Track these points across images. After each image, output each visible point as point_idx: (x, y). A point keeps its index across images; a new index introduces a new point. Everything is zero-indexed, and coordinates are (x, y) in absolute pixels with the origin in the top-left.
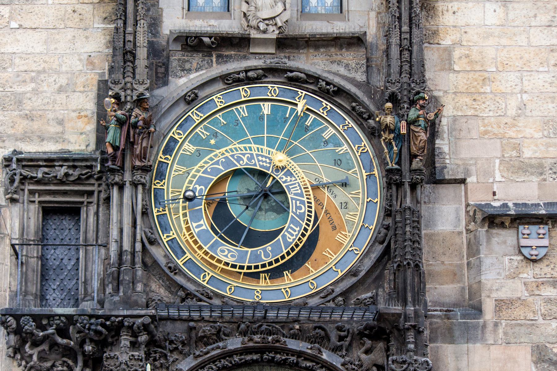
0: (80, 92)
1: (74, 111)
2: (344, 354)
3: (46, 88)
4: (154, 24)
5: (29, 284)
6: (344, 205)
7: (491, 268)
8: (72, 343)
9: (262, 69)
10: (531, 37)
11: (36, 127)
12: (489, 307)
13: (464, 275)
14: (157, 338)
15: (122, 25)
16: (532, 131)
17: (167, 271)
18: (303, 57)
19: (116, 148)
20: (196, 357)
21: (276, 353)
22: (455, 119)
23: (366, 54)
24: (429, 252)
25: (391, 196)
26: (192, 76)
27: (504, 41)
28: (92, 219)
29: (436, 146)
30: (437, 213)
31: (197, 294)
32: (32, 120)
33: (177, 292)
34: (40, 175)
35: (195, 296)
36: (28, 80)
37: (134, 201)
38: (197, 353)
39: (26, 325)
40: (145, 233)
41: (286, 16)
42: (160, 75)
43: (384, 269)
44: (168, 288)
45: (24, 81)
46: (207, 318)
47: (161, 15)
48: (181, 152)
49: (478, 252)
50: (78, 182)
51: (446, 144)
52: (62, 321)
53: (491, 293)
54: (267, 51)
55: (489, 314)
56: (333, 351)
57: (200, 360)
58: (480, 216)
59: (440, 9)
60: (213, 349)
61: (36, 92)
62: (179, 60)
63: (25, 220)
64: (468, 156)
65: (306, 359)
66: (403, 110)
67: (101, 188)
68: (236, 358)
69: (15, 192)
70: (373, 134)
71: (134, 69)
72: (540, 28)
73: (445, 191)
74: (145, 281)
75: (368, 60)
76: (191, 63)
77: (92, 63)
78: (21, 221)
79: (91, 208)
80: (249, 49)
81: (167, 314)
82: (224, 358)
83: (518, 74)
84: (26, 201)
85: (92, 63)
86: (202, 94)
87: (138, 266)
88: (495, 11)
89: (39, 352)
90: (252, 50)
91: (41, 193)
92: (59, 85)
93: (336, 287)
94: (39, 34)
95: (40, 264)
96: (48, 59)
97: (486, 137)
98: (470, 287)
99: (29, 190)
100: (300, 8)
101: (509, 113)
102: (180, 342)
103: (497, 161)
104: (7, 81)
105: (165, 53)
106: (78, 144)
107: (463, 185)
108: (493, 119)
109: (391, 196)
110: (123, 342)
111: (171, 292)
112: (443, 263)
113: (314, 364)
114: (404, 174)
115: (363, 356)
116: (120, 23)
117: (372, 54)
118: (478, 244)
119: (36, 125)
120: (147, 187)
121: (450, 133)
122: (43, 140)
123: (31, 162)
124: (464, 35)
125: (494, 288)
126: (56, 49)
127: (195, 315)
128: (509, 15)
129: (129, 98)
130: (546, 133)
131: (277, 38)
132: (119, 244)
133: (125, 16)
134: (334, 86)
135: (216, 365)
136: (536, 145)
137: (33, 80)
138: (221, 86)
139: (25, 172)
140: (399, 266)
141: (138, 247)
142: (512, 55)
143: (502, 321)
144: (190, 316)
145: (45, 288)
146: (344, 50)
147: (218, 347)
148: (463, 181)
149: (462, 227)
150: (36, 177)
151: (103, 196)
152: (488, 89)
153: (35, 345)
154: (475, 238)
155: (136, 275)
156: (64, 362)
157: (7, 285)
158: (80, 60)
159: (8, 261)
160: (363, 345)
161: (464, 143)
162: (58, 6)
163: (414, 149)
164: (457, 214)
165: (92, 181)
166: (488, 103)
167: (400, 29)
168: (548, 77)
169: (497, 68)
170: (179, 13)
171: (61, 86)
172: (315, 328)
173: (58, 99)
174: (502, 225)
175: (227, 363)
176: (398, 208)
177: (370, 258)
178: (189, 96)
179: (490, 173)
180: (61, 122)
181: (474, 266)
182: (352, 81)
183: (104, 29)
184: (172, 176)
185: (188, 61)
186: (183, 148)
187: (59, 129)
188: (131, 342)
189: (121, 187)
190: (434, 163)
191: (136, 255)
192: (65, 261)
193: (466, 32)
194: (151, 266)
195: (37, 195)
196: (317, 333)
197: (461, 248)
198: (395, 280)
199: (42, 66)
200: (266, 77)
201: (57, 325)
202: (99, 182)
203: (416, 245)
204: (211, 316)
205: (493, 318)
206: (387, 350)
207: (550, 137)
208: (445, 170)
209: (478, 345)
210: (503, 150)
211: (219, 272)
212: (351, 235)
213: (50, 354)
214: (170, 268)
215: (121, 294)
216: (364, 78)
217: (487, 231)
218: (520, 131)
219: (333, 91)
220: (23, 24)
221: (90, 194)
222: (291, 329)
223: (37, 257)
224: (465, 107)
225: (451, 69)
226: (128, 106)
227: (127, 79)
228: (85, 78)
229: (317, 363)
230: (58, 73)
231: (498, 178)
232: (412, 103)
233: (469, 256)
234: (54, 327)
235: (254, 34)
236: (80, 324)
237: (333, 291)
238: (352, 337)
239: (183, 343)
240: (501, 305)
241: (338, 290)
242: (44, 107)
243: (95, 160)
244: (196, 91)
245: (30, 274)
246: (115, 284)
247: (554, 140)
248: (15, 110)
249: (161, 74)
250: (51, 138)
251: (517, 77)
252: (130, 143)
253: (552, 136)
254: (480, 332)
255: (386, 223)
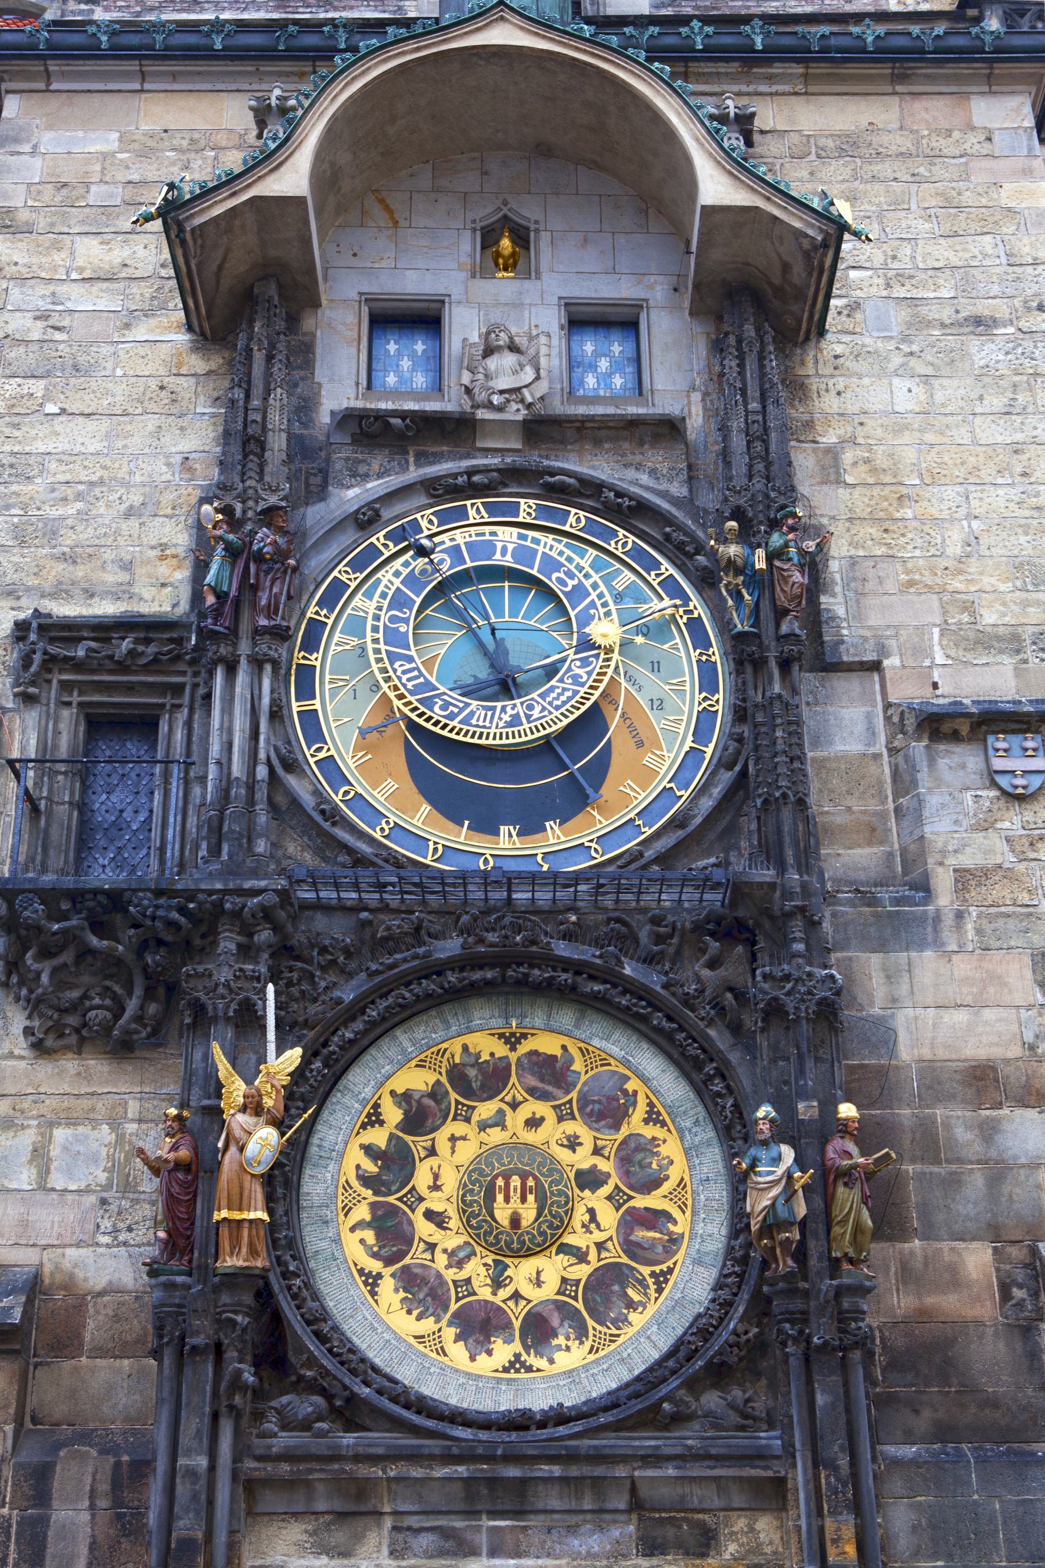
0: (166, 516)
1: (153, 548)
2: (667, 968)
3: (102, 510)
4: (304, 407)
5: (52, 852)
6: (656, 704)
7: (941, 813)
8: (120, 947)
9: (498, 470)
10: (978, 431)
11: (80, 574)
12: (943, 882)
13: (890, 830)
14: (294, 942)
15: (242, 396)
16: (993, 580)
17: (318, 818)
18: (573, 457)
19: (221, 597)
20: (372, 974)
21: (531, 966)
22: (853, 562)
23: (687, 454)
24: (821, 791)
25: (744, 683)
26: (369, 485)
27: (930, 437)
28: (179, 735)
29: (823, 606)
30: (832, 721)
31: (375, 859)
32: (75, 562)
33: (336, 857)
34: (81, 653)
35: (373, 864)
36: (71, 497)
37: (256, 692)
38: (374, 967)
39: (26, 909)
40: (276, 749)
41: (542, 388)
42: (313, 488)
43: (739, 814)
44: (318, 852)
45: (65, 499)
46: (394, 905)
47: (319, 394)
48: (349, 611)
49: (914, 783)
50: (152, 668)
51: (839, 604)
52: (99, 902)
53: (945, 857)
54: (507, 446)
55: (944, 898)
56: (644, 961)
57: (378, 979)
58: (913, 720)
59: (814, 388)
60: (405, 960)
61: (83, 516)
62: (347, 459)
63: (50, 734)
64: (882, 623)
65: (592, 978)
66: (758, 536)
67: (196, 680)
68: (452, 977)
69: (33, 683)
70: (703, 580)
71: (262, 466)
72: (992, 417)
73: (846, 685)
74: (273, 837)
75: (690, 467)
76: (369, 465)
77: (190, 469)
78: (42, 737)
79: (179, 715)
80: (474, 442)
81: (313, 895)
82: (426, 977)
83: (960, 489)
84: (52, 701)
85: (190, 469)
86: (386, 514)
87: (261, 807)
88: (910, 391)
89: (55, 971)
90: (479, 444)
91: (83, 687)
92: (127, 504)
93: (648, 849)
94: (96, 423)
95: (66, 805)
96: (109, 464)
97: (912, 590)
98: (904, 851)
99: (60, 681)
100: (566, 384)
101: (949, 551)
102: (341, 949)
103: (936, 631)
104: (31, 498)
105: (323, 454)
106: (156, 603)
107: (876, 677)
108: (921, 562)
109: (744, 683)
110: (222, 945)
111: (325, 859)
112: (849, 809)
113: (608, 986)
114: (767, 643)
115: (706, 973)
116: (239, 394)
117: (698, 458)
118: (914, 769)
119: (80, 572)
120: (283, 671)
121: (846, 586)
122: (92, 596)
123: (68, 631)
124: (860, 428)
125: (950, 848)
126: (125, 446)
127: (372, 898)
128: (936, 397)
129: (250, 514)
130: (1018, 583)
131: (525, 421)
132: (225, 771)
133: (249, 382)
134: (631, 499)
135: (411, 991)
136: (1004, 604)
137: (79, 497)
138: (424, 500)
139: (53, 650)
140: (766, 802)
141: (262, 772)
142: (946, 459)
143: (971, 909)
144: (360, 899)
145: (86, 864)
146: (646, 447)
147: (416, 957)
148: (875, 666)
149: (880, 745)
150: (73, 658)
151: (202, 691)
152: (909, 513)
153: (45, 953)
154: (906, 762)
155: (255, 823)
156: (107, 989)
157: (7, 851)
158: (168, 465)
159: (11, 809)
160: (704, 951)
161: (871, 601)
162: (134, 379)
163: (782, 600)
164: (870, 722)
165: (182, 667)
166: (910, 536)
167: (746, 404)
168: (1014, 493)
169: (922, 480)
170: (351, 392)
171: (131, 507)
172: (609, 920)
173: (124, 526)
174: (955, 737)
175: (433, 987)
176: (759, 698)
177: (711, 796)
178: (364, 514)
179: (922, 650)
180: (127, 566)
181: (910, 814)
182: (664, 495)
183: (213, 415)
184: (331, 653)
185: (363, 461)
186: (352, 605)
187: (123, 577)
188: (239, 946)
189: (231, 670)
190: (820, 635)
191: (257, 787)
192: (127, 815)
193: (861, 424)
194: (287, 810)
195: (75, 693)
196: (612, 930)
197: (880, 783)
198: (759, 829)
199: (98, 474)
200: (506, 485)
201: (89, 910)
202: (196, 669)
203: (796, 765)
204: (402, 900)
205: (952, 902)
206: (754, 958)
207: (1028, 591)
208: (842, 648)
209: (928, 954)
210: (945, 613)
211: (419, 824)
212: (672, 756)
213: (77, 974)
214: (323, 812)
215: (225, 856)
216: (684, 491)
217: (927, 747)
218: (972, 581)
219: (629, 507)
220: (67, 407)
221: (177, 690)
222: (562, 924)
223: (70, 803)
224: (870, 543)
225: (839, 482)
226: (249, 527)
227: (248, 483)
228: (175, 494)
229: (615, 986)
230: (126, 485)
231: (940, 659)
232: (774, 524)
233: (896, 796)
234: (83, 915)
235: (481, 414)
236: (136, 906)
237: (642, 855)
238: (682, 936)
239: (348, 953)
240: (964, 878)
241: (649, 854)
242: (97, 542)
243: (187, 627)
244: (377, 506)
245: (54, 833)
246: (213, 841)
247: (1034, 595)
248: (43, 547)
249: (315, 484)
250: (107, 592)
251: (958, 493)
252: (249, 588)
253: (1030, 587)
254: (929, 929)
255: (737, 730)
